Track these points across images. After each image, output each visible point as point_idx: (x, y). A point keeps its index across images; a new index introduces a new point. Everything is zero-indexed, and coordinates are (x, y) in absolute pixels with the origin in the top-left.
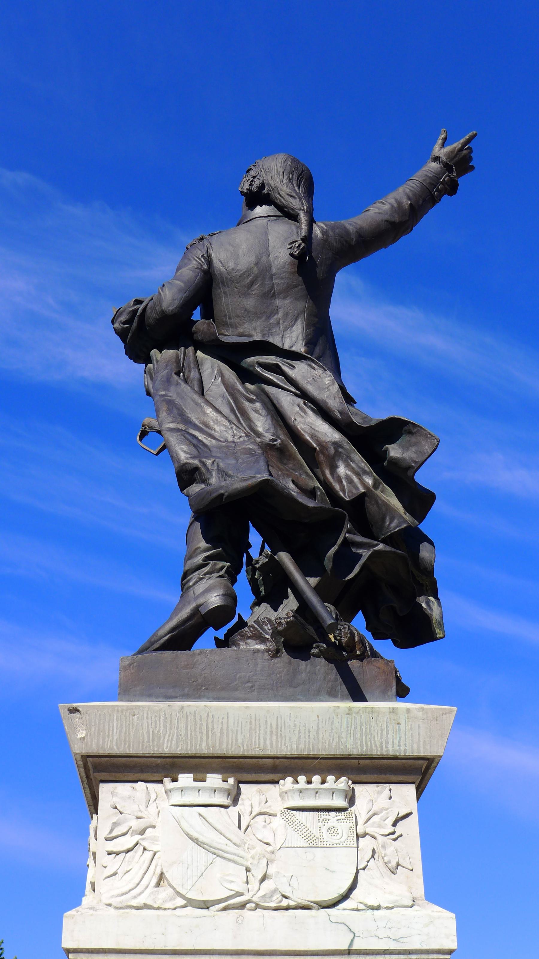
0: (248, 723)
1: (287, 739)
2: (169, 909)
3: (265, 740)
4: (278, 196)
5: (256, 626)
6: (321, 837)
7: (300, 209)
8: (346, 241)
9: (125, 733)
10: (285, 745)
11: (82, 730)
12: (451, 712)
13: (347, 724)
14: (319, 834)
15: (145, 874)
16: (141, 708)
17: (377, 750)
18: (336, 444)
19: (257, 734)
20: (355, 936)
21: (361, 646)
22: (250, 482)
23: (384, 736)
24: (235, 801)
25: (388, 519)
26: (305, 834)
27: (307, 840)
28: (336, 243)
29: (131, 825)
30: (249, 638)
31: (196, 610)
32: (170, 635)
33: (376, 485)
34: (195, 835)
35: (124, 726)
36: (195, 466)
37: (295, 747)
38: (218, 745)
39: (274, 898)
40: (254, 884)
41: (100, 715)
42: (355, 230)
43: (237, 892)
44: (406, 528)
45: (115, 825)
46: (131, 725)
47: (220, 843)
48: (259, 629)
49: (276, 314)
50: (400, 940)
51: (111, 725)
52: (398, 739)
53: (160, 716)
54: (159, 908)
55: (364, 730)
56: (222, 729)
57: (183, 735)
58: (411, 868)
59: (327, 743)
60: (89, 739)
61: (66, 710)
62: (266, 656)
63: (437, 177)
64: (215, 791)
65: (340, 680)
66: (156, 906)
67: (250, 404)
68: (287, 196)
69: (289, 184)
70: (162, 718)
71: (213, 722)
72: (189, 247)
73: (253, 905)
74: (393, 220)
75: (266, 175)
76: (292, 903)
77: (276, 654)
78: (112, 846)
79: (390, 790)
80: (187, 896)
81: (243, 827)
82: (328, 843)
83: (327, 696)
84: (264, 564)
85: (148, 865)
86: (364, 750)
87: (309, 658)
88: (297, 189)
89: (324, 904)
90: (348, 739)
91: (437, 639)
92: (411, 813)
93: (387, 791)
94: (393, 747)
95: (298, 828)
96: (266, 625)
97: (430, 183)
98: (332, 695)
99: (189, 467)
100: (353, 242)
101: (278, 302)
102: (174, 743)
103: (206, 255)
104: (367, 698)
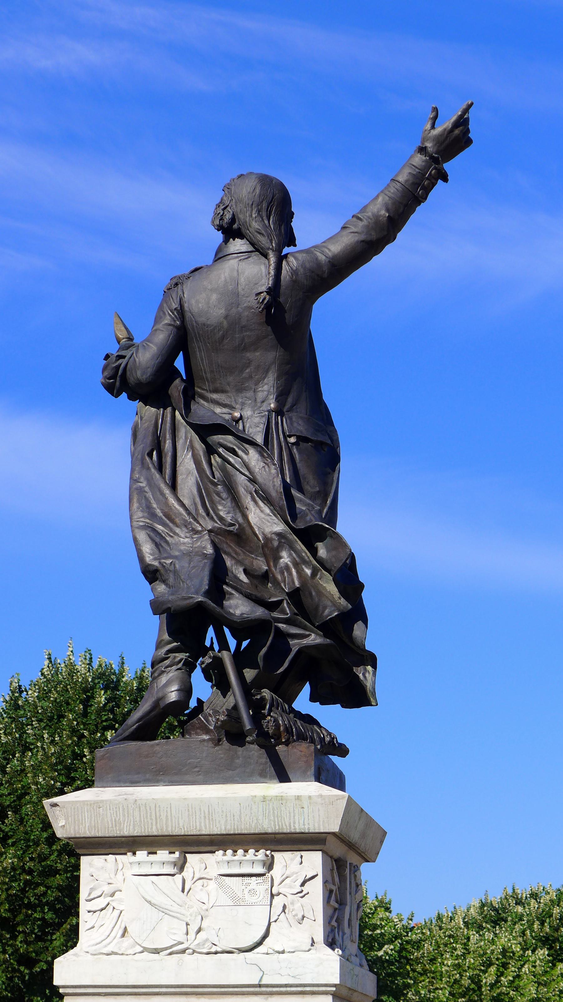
0: (187, 811)
1: (217, 822)
2: (130, 954)
3: (200, 823)
4: (248, 231)
5: (203, 719)
6: (244, 898)
7: (269, 249)
8: (318, 275)
9: (94, 821)
10: (216, 826)
11: (63, 819)
12: (343, 797)
13: (263, 809)
14: (242, 895)
15: (114, 927)
16: (105, 802)
17: (287, 828)
18: (279, 535)
19: (194, 819)
20: (263, 974)
21: (286, 734)
22: (188, 601)
23: (292, 818)
24: (182, 869)
25: (321, 608)
26: (231, 896)
27: (233, 900)
28: (307, 280)
29: (104, 890)
30: (198, 728)
32: (137, 725)
33: (314, 574)
34: (149, 898)
35: (93, 815)
36: (155, 568)
37: (223, 828)
38: (165, 827)
39: (206, 946)
41: (74, 809)
43: (179, 942)
44: (336, 615)
45: (92, 890)
46: (98, 815)
47: (166, 905)
48: (205, 722)
49: (248, 367)
50: (297, 977)
51: (83, 815)
52: (303, 819)
53: (119, 807)
54: (122, 954)
55: (276, 813)
56: (167, 816)
57: (138, 821)
58: (314, 919)
59: (248, 824)
60: (68, 827)
61: (49, 805)
62: (211, 744)
63: (422, 174)
64: (164, 863)
65: (269, 763)
67: (213, 487)
68: (256, 233)
70: (121, 809)
71: (160, 810)
72: (166, 291)
73: (191, 951)
74: (369, 239)
75: (236, 206)
76: (219, 949)
79: (302, 857)
80: (143, 945)
81: (186, 891)
82: (248, 902)
83: (258, 777)
84: (209, 664)
85: (116, 921)
86: (277, 828)
87: (245, 745)
88: (266, 222)
89: (243, 949)
90: (264, 820)
91: (372, 705)
92: (317, 875)
94: (299, 826)
95: (226, 891)
96: (211, 716)
98: (262, 777)
99: (151, 569)
100: (325, 275)
101: (249, 355)
102: (131, 827)
103: (179, 308)
104: (291, 777)
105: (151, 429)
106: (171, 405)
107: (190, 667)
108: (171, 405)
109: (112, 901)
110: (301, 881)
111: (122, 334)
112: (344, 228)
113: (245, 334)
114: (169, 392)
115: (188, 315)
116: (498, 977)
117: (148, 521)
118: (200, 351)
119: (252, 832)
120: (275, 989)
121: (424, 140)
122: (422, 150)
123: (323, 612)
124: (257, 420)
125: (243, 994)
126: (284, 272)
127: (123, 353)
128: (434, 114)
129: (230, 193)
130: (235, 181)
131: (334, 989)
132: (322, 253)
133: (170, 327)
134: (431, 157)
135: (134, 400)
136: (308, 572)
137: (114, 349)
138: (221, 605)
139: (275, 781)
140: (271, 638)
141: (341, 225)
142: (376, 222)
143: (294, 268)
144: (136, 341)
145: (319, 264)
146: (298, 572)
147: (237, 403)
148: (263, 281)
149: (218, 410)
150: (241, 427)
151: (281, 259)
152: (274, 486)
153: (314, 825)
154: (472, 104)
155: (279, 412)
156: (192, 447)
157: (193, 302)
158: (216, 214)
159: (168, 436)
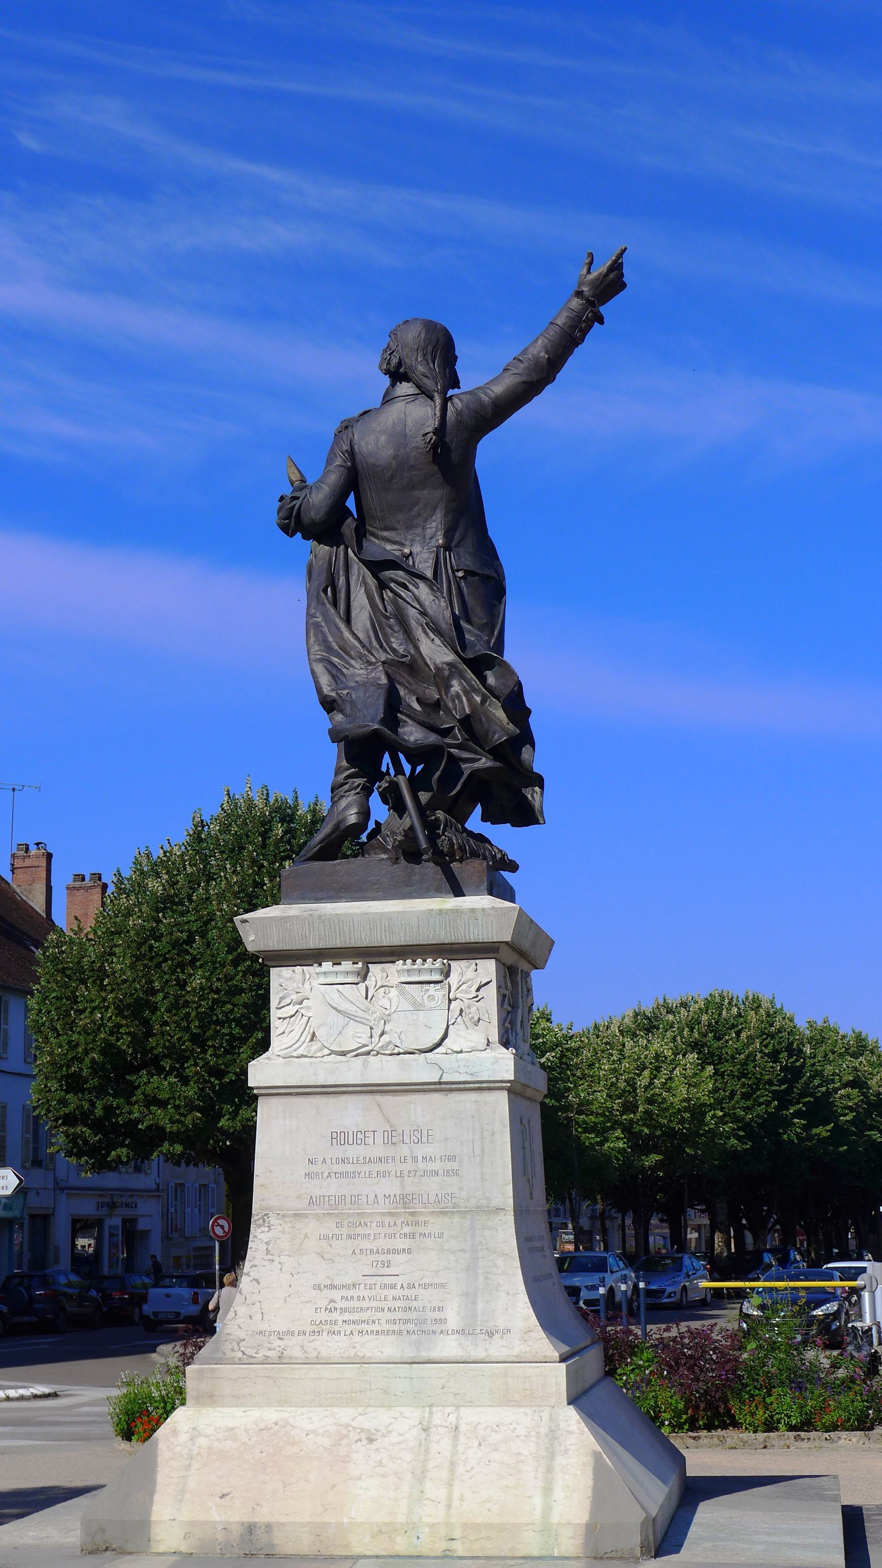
7: (434, 391)
8: (481, 416)
12: (514, 908)
15: (303, 1033)
18: (450, 665)
22: (365, 729)
23: (467, 929)
24: (365, 978)
25: (490, 733)
30: (377, 848)
31: (337, 826)
33: (483, 701)
34: (335, 1005)
40: (376, 1039)
41: (263, 924)
42: (491, 401)
45: (282, 999)
54: (312, 1057)
56: (350, 929)
62: (389, 863)
65: (445, 879)
66: (310, 1055)
69: (424, 362)
73: (375, 1052)
76: (401, 1051)
77: (396, 861)
78: (280, 1013)
79: (476, 965)
81: (369, 999)
88: (432, 365)
91: (540, 824)
93: (473, 966)
96: (389, 837)
97: (571, 326)
98: (438, 892)
99: (329, 699)
101: (417, 493)
105: (325, 566)
106: (344, 543)
107: (367, 791)
108: (344, 543)
109: (301, 1008)
110: (476, 987)
111: (295, 477)
112: (506, 370)
113: (413, 473)
114: (342, 531)
115: (358, 457)
116: (652, 1079)
117: (325, 654)
118: (370, 491)
119: (430, 943)
120: (454, 1086)
121: (580, 284)
122: (579, 294)
123: (493, 737)
124: (426, 556)
125: (424, 1091)
126: (449, 413)
127: (297, 494)
128: (590, 259)
129: (396, 338)
130: (401, 327)
131: (509, 1085)
132: (486, 394)
133: (343, 468)
134: (588, 301)
135: (308, 539)
136: (478, 699)
137: (288, 491)
138: (396, 732)
139: (450, 896)
140: (444, 762)
141: (503, 368)
142: (536, 364)
143: (459, 409)
144: (309, 482)
145: (482, 405)
146: (468, 700)
147: (406, 540)
148: (430, 422)
149: (389, 547)
150: (411, 563)
151: (446, 400)
152: (444, 617)
153: (488, 936)
154: (626, 249)
155: (447, 547)
156: (365, 583)
157: (363, 443)
158: (383, 359)
159: (341, 573)
